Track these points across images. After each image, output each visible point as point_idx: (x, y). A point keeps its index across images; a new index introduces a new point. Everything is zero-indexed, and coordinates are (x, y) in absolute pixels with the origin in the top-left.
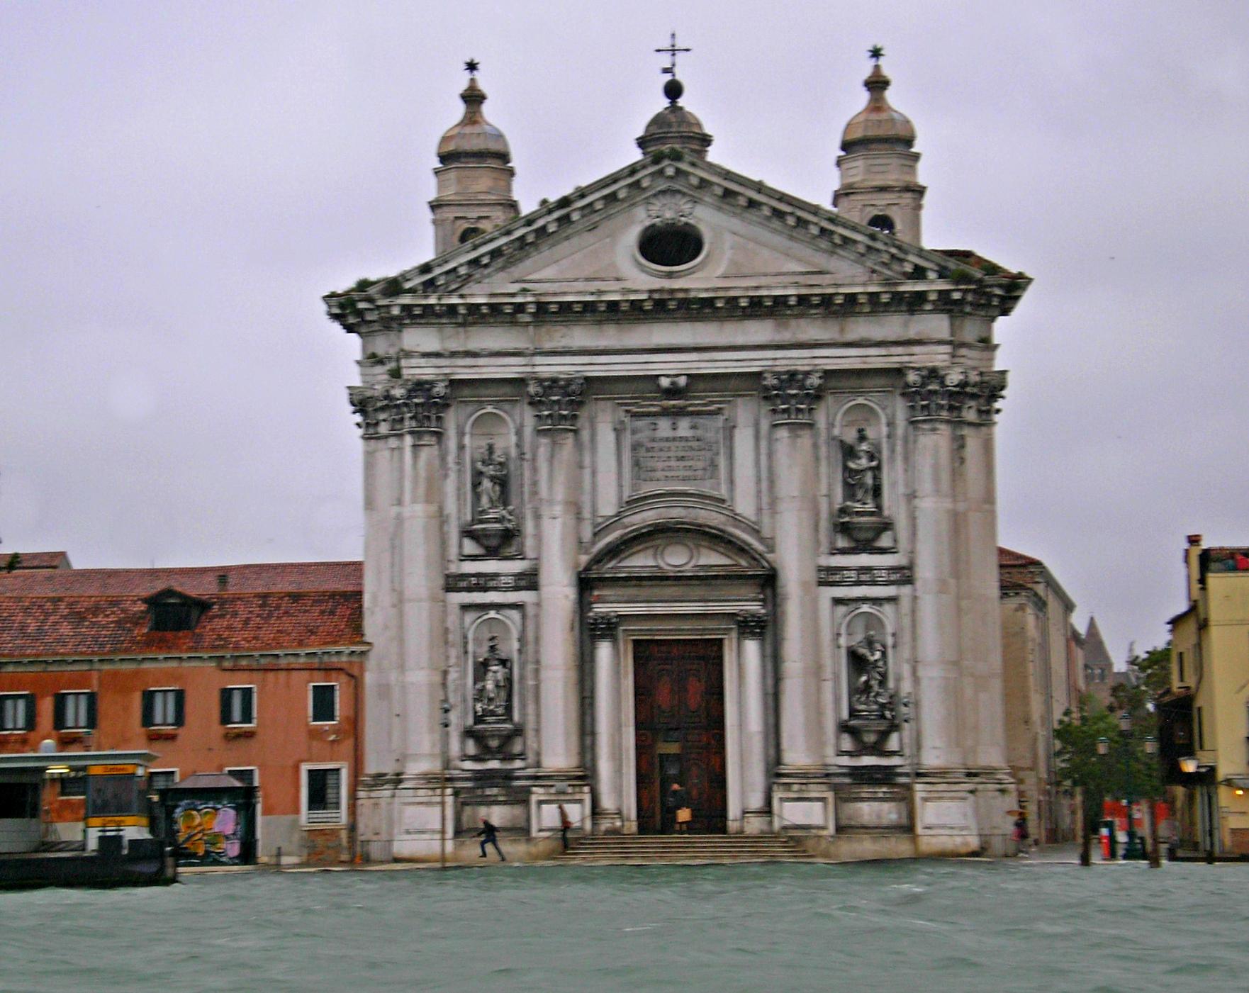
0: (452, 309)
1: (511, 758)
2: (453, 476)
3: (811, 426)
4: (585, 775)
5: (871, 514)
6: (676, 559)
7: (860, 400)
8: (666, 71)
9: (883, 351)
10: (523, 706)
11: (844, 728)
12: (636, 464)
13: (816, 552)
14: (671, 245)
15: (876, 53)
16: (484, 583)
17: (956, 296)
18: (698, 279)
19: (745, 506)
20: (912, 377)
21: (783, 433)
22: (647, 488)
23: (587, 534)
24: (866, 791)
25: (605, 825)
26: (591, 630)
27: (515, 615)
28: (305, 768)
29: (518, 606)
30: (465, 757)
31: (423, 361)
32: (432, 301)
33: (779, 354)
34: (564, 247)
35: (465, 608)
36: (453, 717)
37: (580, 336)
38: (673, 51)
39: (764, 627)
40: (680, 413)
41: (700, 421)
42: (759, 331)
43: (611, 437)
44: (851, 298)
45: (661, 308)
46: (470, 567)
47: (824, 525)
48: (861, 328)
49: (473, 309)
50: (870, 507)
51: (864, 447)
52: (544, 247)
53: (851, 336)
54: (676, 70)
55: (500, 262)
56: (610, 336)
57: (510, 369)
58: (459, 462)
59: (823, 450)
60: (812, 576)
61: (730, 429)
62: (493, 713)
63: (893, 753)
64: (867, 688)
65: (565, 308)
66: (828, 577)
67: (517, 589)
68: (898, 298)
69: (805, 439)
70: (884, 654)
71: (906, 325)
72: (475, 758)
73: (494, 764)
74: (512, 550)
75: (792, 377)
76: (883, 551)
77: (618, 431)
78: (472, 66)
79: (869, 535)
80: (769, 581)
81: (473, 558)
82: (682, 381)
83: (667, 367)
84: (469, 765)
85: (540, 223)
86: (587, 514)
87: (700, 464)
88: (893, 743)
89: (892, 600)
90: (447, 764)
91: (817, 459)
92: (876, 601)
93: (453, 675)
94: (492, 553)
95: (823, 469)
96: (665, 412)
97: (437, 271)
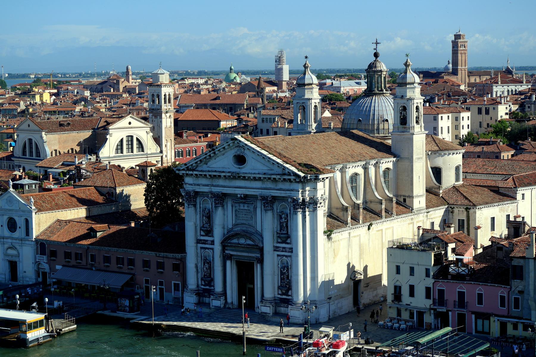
0: (192, 175)
1: (211, 286)
2: (198, 214)
3: (272, 209)
4: (224, 293)
5: (285, 234)
6: (242, 241)
7: (284, 203)
8: (375, 49)
9: (284, 192)
10: (213, 274)
11: (279, 288)
12: (236, 215)
13: (273, 243)
14: (240, 160)
15: (407, 55)
16: (205, 242)
17: (298, 180)
18: (246, 169)
19: (259, 229)
20: (289, 200)
21: (264, 212)
22: (238, 222)
23: (226, 232)
24: (282, 305)
25: (227, 306)
26: (225, 258)
27: (211, 251)
28: (173, 282)
29: (212, 249)
30: (202, 285)
31: (189, 186)
32: (187, 172)
33: (263, 191)
34: (218, 159)
35: (201, 248)
36: (199, 275)
37: (221, 182)
38: (377, 43)
39: (261, 261)
40: (244, 203)
41: (249, 205)
42: (258, 184)
43: (231, 207)
44: (274, 179)
45: (234, 178)
46: (202, 238)
47: (275, 235)
48: (281, 185)
49: (196, 175)
50: (284, 232)
51: (283, 216)
52: (213, 159)
53: (278, 187)
54: (377, 49)
55: (203, 163)
56: (227, 183)
57: (206, 189)
58: (200, 211)
59: (276, 215)
60: (273, 249)
61: (255, 208)
62: (206, 275)
63: (289, 296)
64: (284, 279)
65: (215, 176)
66: (276, 249)
67: (212, 244)
68: (284, 179)
69: (270, 214)
70: (288, 270)
71: (290, 185)
72: (204, 285)
73: (208, 287)
74: (210, 235)
75: (264, 198)
76: (288, 243)
77: (232, 206)
78: (306, 57)
79: (284, 239)
80: (261, 250)
81: (203, 236)
82: (242, 196)
83: (239, 191)
84: (203, 287)
85: (209, 154)
86: (226, 227)
87: (249, 217)
88: (290, 293)
89: (290, 256)
90: (198, 286)
91: (274, 217)
92: (286, 256)
93: (199, 265)
94: (207, 235)
95: (276, 221)
96: (241, 203)
97: (188, 165)
